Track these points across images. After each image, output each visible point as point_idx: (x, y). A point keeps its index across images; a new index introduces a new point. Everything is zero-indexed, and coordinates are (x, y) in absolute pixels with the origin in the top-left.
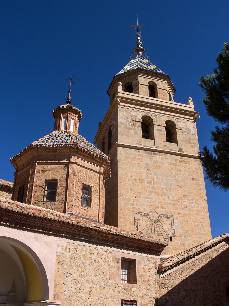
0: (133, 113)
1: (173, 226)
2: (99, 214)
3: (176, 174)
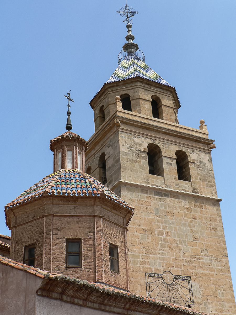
0: (137, 140)
1: (191, 290)
2: (127, 281)
3: (191, 222)
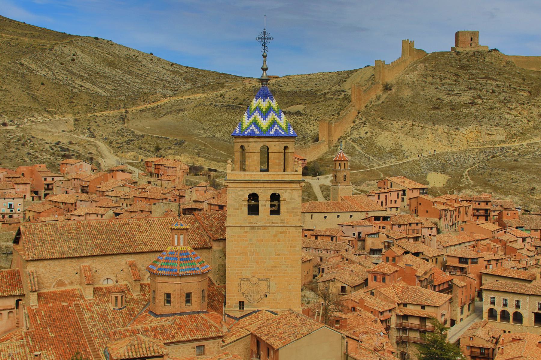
0: (241, 193)
